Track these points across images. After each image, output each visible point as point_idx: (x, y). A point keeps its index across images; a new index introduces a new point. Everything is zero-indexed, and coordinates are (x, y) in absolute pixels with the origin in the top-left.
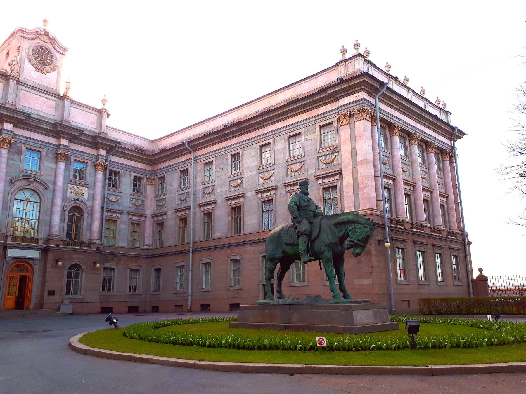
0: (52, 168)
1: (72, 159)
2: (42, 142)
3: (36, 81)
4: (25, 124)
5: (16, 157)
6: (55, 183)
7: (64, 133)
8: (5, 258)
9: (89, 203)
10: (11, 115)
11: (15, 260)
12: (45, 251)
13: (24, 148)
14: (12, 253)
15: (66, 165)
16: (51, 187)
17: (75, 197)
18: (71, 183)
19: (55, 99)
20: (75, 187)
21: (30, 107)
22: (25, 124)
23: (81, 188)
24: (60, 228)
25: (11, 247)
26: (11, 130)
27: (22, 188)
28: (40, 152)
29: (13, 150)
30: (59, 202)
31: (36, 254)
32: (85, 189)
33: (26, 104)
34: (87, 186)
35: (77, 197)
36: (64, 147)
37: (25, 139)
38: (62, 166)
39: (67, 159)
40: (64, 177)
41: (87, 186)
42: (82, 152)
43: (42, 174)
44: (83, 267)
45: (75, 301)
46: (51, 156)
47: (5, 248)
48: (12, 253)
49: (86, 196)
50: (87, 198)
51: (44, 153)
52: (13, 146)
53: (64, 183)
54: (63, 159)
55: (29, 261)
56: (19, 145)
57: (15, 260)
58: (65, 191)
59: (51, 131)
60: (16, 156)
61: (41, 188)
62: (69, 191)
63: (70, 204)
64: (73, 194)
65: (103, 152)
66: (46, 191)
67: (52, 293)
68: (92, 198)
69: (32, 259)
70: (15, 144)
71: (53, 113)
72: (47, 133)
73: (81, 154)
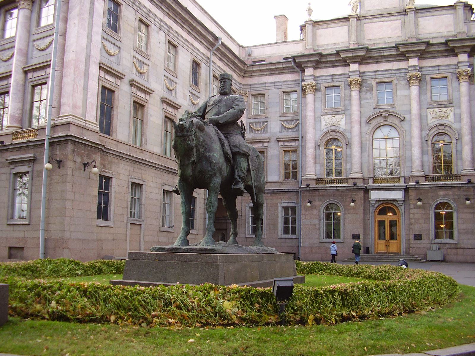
0: (406, 96)
1: (428, 78)
2: (391, 70)
3: (378, 8)
4: (370, 58)
5: (368, 95)
6: (410, 112)
7: (408, 52)
8: (370, 202)
9: (456, 126)
10: (351, 55)
11: (380, 203)
12: (406, 190)
13: (374, 84)
14: (374, 195)
15: (420, 87)
16: (407, 117)
17: (436, 122)
18: (431, 106)
19: (399, 17)
20: (436, 110)
21: (376, 37)
22: (370, 58)
23: (444, 109)
24: (422, 162)
25: (372, 190)
26: (357, 69)
27: (379, 125)
28: (391, 82)
29: (364, 89)
30: (416, 132)
31: (398, 195)
32: (449, 109)
33: (371, 37)
34: (451, 105)
35: (440, 122)
36: (413, 68)
37: (374, 74)
38: (415, 89)
39: (420, 80)
40: (420, 103)
41: (451, 105)
42: (438, 66)
43: (396, 105)
44: (453, 206)
45: (447, 246)
46: (403, 82)
47: (367, 191)
48: (374, 195)
49: (451, 118)
50: (453, 121)
51: (395, 82)
52: (364, 84)
53: (420, 109)
54: (414, 81)
55: (394, 203)
56: (369, 82)
57: (380, 203)
58: (422, 119)
59: (398, 55)
60: (368, 93)
61: (396, 122)
62: (430, 117)
63: (432, 132)
64: (435, 120)
65: (463, 57)
66: (402, 123)
67: (418, 237)
68: (458, 118)
69: (395, 200)
70: (366, 82)
71: (400, 34)
72: (394, 58)
73: (437, 68)
